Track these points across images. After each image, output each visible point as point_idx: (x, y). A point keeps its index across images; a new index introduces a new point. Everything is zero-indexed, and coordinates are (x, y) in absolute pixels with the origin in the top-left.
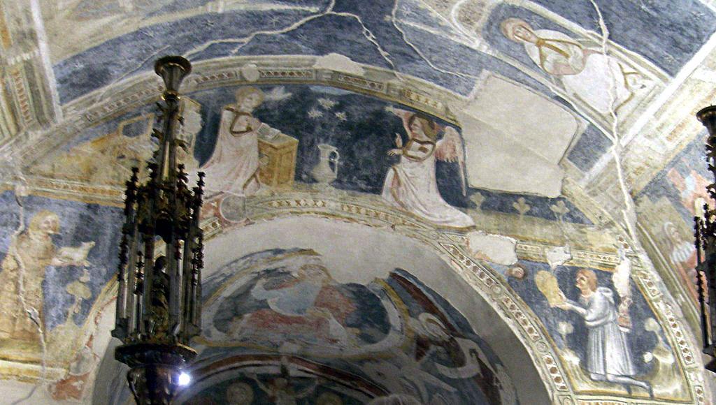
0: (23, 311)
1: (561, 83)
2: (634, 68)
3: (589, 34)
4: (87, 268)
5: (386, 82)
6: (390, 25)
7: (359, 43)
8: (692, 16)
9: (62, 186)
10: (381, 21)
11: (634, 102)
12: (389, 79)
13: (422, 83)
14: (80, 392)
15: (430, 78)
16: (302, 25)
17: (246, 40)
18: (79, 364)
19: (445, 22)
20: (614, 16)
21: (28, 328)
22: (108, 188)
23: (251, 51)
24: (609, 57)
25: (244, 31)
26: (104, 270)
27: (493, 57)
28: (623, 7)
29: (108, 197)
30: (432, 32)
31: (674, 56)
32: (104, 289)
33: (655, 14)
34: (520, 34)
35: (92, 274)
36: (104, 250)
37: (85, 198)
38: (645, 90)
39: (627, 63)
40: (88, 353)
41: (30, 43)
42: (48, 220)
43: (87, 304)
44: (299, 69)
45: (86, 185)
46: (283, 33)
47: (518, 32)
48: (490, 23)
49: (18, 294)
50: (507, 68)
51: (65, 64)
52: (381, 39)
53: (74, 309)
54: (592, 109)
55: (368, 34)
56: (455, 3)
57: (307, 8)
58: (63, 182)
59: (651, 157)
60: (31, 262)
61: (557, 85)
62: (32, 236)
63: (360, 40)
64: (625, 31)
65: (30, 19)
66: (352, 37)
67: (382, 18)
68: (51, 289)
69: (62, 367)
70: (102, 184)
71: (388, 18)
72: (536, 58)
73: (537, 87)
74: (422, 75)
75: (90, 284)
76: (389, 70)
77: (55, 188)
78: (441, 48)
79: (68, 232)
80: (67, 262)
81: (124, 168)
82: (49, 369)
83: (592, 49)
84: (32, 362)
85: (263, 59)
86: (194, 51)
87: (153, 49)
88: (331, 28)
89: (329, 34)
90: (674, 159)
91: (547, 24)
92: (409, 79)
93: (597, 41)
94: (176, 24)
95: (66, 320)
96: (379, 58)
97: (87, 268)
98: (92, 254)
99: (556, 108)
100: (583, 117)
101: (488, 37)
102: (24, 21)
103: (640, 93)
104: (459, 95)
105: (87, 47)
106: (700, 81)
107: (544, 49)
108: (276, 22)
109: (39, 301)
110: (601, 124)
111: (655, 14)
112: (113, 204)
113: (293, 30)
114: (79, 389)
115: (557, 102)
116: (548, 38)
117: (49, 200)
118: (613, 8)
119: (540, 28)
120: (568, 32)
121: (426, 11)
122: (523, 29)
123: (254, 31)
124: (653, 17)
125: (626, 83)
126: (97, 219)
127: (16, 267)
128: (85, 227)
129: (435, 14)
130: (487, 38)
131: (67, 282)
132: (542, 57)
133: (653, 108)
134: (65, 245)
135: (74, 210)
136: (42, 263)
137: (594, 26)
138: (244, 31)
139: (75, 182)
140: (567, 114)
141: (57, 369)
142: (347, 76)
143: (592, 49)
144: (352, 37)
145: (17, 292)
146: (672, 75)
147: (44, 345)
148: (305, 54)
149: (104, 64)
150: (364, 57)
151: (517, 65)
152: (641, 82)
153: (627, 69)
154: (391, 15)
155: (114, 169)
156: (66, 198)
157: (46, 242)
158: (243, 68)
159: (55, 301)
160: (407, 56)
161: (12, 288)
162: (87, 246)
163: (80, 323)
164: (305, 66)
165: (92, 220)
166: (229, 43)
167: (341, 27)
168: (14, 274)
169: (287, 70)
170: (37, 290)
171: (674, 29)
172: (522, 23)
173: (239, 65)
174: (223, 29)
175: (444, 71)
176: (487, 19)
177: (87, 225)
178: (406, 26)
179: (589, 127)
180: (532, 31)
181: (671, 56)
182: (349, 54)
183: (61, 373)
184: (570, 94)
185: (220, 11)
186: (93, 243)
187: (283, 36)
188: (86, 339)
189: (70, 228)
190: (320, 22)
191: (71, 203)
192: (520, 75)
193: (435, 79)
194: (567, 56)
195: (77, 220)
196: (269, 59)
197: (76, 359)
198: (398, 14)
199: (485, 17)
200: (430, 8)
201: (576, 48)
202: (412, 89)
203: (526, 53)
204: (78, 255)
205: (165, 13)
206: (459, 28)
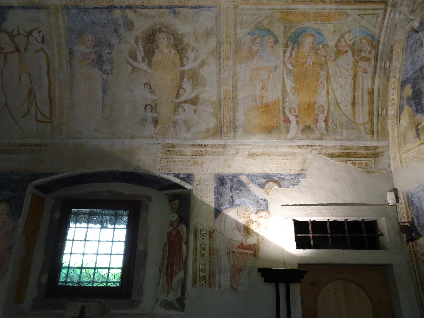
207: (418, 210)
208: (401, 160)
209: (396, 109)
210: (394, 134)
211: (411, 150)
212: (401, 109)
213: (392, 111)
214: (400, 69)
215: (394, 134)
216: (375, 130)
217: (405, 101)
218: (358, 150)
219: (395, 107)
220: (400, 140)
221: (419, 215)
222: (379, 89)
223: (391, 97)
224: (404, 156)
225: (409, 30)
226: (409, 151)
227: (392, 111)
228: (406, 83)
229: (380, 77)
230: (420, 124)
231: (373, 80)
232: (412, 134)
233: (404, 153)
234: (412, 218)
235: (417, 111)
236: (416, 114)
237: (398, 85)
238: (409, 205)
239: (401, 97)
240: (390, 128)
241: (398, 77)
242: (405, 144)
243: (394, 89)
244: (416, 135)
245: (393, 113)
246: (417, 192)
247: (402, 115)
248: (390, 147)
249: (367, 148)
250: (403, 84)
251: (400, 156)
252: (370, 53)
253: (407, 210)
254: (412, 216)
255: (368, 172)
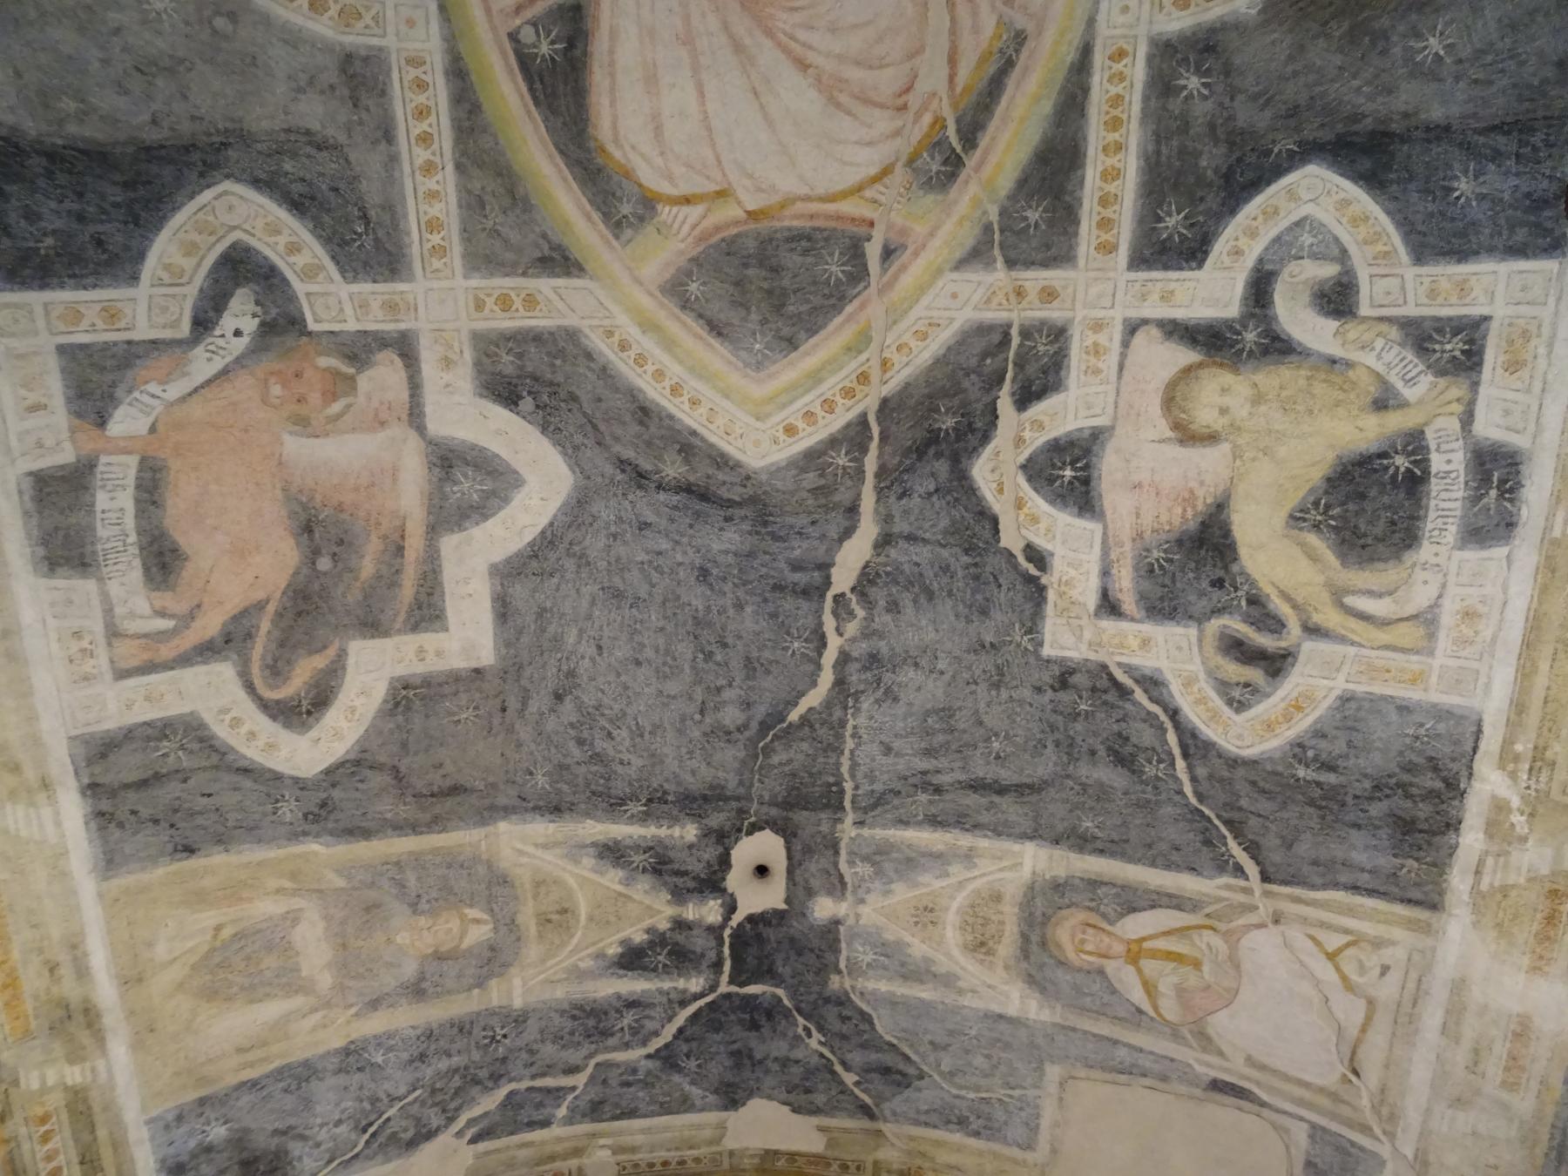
1: (1209, 1039)
2: (1347, 931)
3: (1219, 887)
5: (870, 1159)
6: (842, 1001)
7: (797, 1062)
8: (1408, 740)
10: (827, 993)
11: (1382, 1024)
12: (876, 1148)
13: (938, 1144)
15: (949, 1122)
16: (681, 1031)
17: (580, 1080)
19: (943, 965)
20: (1253, 822)
23: (594, 1111)
24: (1281, 928)
25: (573, 1056)
27: (1055, 1025)
28: (1264, 791)
30: (924, 995)
31: (1417, 859)
33: (1331, 778)
34: (1089, 947)
38: (1394, 977)
39: (1323, 925)
41: (85, 1037)
44: (695, 1152)
46: (649, 1056)
47: (1083, 942)
48: (1025, 938)
50: (1090, 1046)
51: (180, 1118)
52: (837, 1043)
54: (1301, 1083)
55: (809, 1035)
56: (947, 909)
57: (681, 983)
59: (1492, 1161)
61: (1204, 1050)
63: (798, 1054)
64: (1290, 847)
65: (83, 972)
66: (779, 1048)
67: (825, 983)
71: (835, 983)
72: (1138, 996)
73: (1163, 1074)
74: (934, 1118)
76: (866, 1124)
78: (951, 1033)
83: (1241, 922)
85: (620, 1133)
86: (476, 1111)
87: (386, 1100)
88: (738, 1032)
89: (735, 1047)
90: (1552, 1138)
91: (1132, 901)
92: (912, 1139)
93: (1241, 898)
94: (429, 1035)
96: (842, 1092)
99: (1223, 1112)
100: (1285, 1112)
101: (1030, 975)
102: (66, 971)
103: (1387, 990)
104: (1015, 1152)
105: (233, 1080)
106: (1505, 891)
107: (1149, 966)
108: (630, 1028)
110: (1334, 1116)
111: (1331, 778)
113: (667, 1046)
115: (1219, 1097)
116: (1144, 933)
118: (1244, 803)
119: (1122, 915)
120: (1176, 902)
121: (900, 945)
122: (1090, 931)
123: (591, 1056)
124: (1333, 787)
125: (1344, 978)
129: (918, 948)
130: (1031, 980)
132: (1149, 988)
133: (1432, 1017)
137: (1225, 865)
138: (573, 1056)
140: (1246, 1121)
142: (792, 1156)
143: (1241, 922)
144: (779, 1048)
146: (1434, 906)
148: (702, 1110)
149: (276, 1132)
150: (811, 1097)
151: (1104, 1028)
152: (1374, 961)
153: (1334, 941)
154: (840, 972)
158: (585, 1161)
160: (894, 1074)
164: (711, 1143)
166: (548, 1091)
167: (754, 1026)
169: (673, 1156)
171: (1388, 792)
172: (1082, 916)
173: (577, 1152)
174: (532, 1052)
175: (972, 1095)
176: (1016, 929)
178: (874, 992)
179: (1311, 1137)
180: (1108, 928)
181: (1411, 863)
182: (784, 1096)
184: (1239, 1063)
185: (518, 1003)
187: (650, 1064)
190: (712, 1017)
192: (1122, 1053)
193: (962, 1122)
194: (1197, 964)
196: (635, 1130)
198: (854, 969)
199: (1011, 931)
200: (908, 938)
201: (1208, 936)
202: (927, 1165)
203: (1114, 992)
205: (403, 1000)
206: (969, 969)
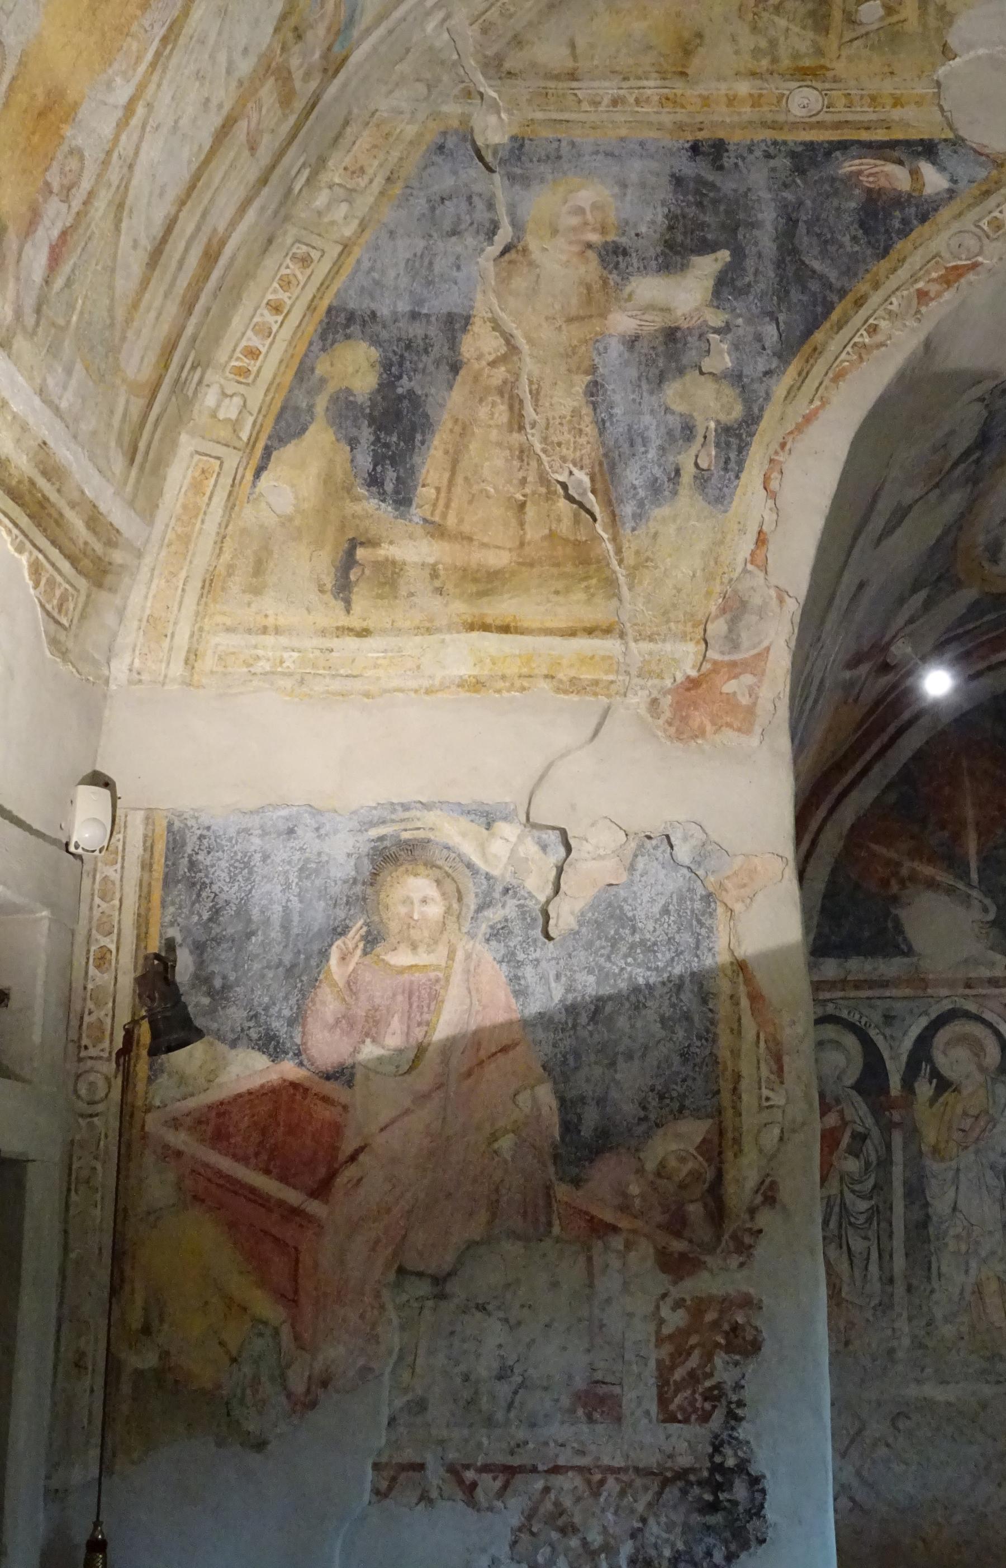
0: (543, 479)
4: (716, 331)
9: (606, 101)
14: (750, 711)
18: (733, 623)
21: (565, 527)
22: (744, 88)
26: (770, 332)
29: (747, 112)
32: (780, 388)
35: (736, 347)
36: (762, 274)
37: (681, 127)
40: (759, 589)
42: (573, 208)
43: (735, 439)
45: (679, 87)
49: (521, 428)
53: (699, 455)
58: (608, 88)
60: (546, 333)
62: (536, 255)
68: (619, 400)
69: (684, 637)
70: (721, 78)
75: (736, 378)
77: (585, 106)
79: (643, 229)
80: (656, 322)
81: (782, 22)
82: (646, 646)
84: (590, 631)
95: (675, 493)
97: (716, 331)
98: (726, 286)
109: (587, 444)
112: (768, 135)
114: (745, 700)
117: (573, 144)
126: (728, 185)
127: (503, 350)
128: (692, 211)
131: (661, 378)
134: (644, 269)
135: (654, 165)
136: (576, 332)
139: (645, 83)
141: (668, 647)
145: (517, 422)
147: (621, 573)
155: (754, 29)
156: (623, 132)
157: (582, 270)
159: (634, 439)
161: (502, 413)
162: (707, 267)
163: (720, 500)
165: (713, 186)
168: (501, 373)
170: (575, 412)
177: (700, 205)
183: (685, 657)
186: (724, 255)
188: (746, 545)
189: (649, 219)
191: (642, 144)
195: (665, 192)
197: (723, 611)
204: (686, 294)
207: (216, 912)
208: (192, 657)
209: (254, 405)
210: (192, 513)
211: (278, 631)
212: (286, 426)
213: (230, 400)
214: (346, 247)
215: (192, 513)
216: (142, 446)
217: (321, 403)
218: (73, 505)
219: (256, 397)
220: (226, 557)
221: (218, 940)
222: (233, 258)
223: (241, 330)
224: (225, 641)
225: (455, 123)
226: (265, 630)
227: (230, 400)
228: (355, 329)
229: (263, 209)
230: (372, 543)
231: (242, 209)
232: (309, 564)
233: (229, 630)
234: (170, 945)
235: (374, 481)
236: (362, 491)
237: (311, 308)
238: (169, 881)
239: (303, 372)
240: (178, 475)
241: (323, 268)
242: (256, 591)
243: (276, 308)
244: (329, 582)
245: (230, 410)
246: (247, 831)
247: (288, 452)
248: (148, 560)
249: (95, 520)
250: (339, 323)
251: (197, 634)
252: (307, 76)
253: (145, 896)
254: (172, 932)
255: (54, 642)
